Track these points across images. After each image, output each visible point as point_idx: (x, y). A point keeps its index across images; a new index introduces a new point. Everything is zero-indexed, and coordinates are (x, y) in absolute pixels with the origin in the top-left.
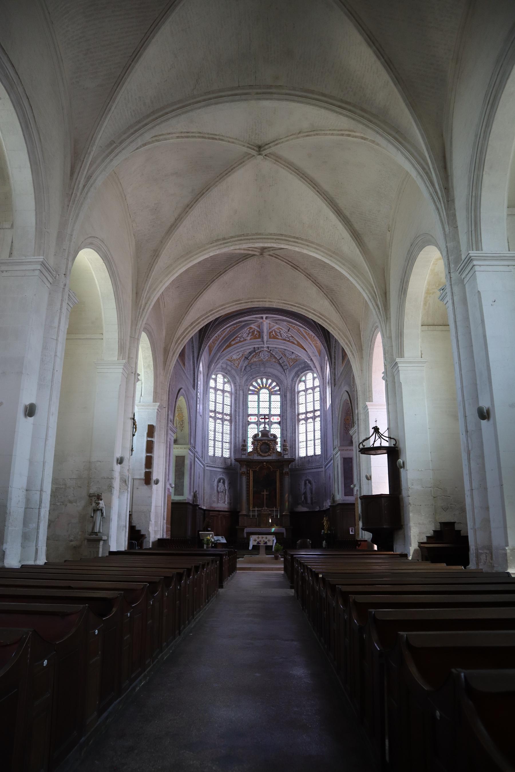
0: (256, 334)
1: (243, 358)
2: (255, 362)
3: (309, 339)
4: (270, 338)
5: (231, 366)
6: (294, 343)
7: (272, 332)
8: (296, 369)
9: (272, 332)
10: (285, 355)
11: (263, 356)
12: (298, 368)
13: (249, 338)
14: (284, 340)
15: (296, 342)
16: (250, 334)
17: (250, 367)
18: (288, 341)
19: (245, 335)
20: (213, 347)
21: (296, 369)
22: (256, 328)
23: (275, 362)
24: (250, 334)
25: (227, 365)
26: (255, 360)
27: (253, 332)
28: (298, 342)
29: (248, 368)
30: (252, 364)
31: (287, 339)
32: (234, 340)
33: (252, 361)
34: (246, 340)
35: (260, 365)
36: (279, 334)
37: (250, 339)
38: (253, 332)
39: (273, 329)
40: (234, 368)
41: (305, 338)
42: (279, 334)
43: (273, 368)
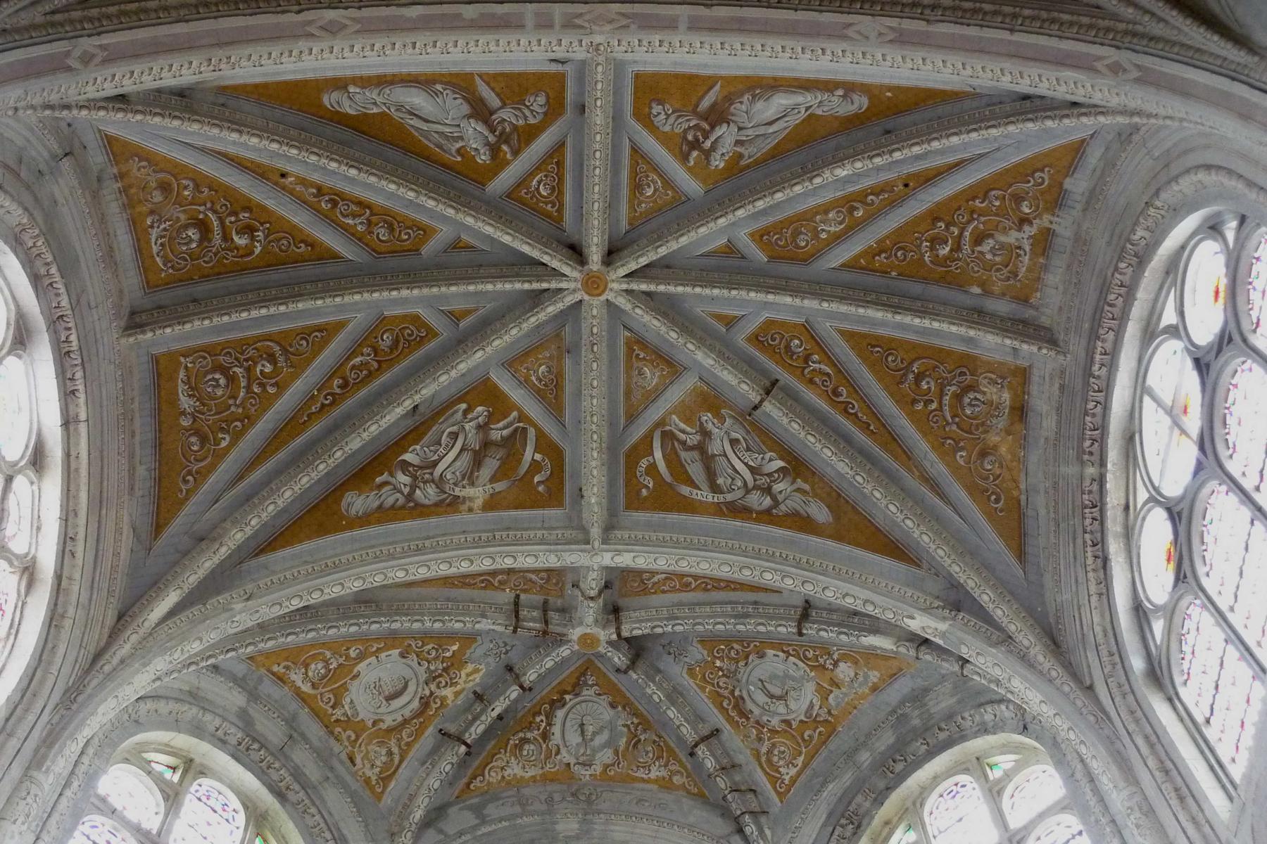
0: (535, 467)
1: (429, 736)
2: (519, 783)
3: (921, 446)
4: (634, 501)
5: (323, 757)
6: (802, 523)
7: (644, 446)
8: (833, 790)
9: (644, 446)
10: (739, 704)
11: (574, 738)
12: (847, 779)
13: (477, 494)
14: (736, 510)
15: (820, 513)
16: (491, 465)
17: (478, 810)
18: (767, 516)
19: (451, 462)
20: (201, 476)
21: (833, 790)
22: (533, 409)
23: (666, 784)
24: (491, 465)
25: (294, 734)
26: (515, 770)
27: (514, 441)
28: (837, 499)
29: (459, 819)
30: (491, 796)
31: (758, 501)
32: (365, 472)
33: (493, 777)
34: (451, 504)
35: (550, 801)
36: (696, 470)
37: (491, 504)
38: (514, 441)
39: (654, 414)
40: (355, 786)
41: (892, 440)
42: (696, 470)
43: (650, 817)
